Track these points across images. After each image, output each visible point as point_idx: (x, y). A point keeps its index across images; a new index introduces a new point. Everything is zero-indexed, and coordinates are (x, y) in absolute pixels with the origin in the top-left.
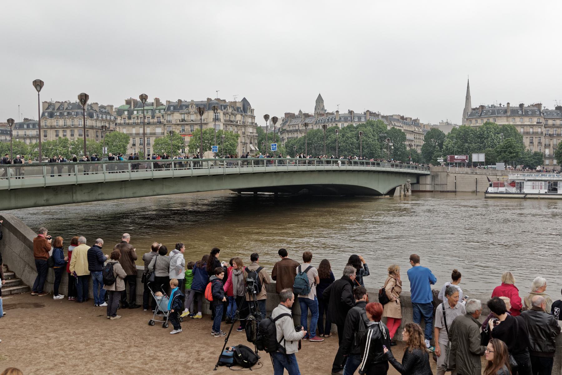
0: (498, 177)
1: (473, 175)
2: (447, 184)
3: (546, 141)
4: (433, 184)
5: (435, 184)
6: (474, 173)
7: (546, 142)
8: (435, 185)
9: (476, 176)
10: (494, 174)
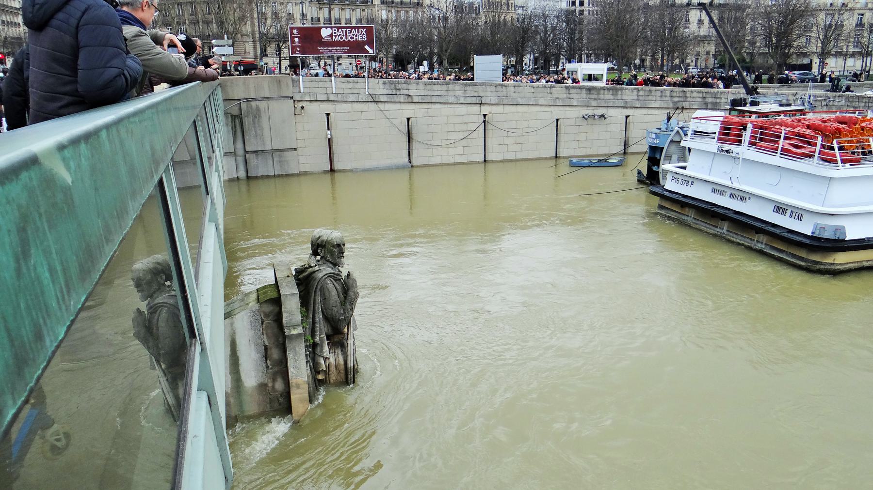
0: (485, 110)
1: (398, 106)
2: (295, 149)
3: (313, 10)
4: (240, 152)
5: (246, 152)
6: (402, 99)
7: (313, 14)
8: (251, 157)
9: (408, 110)
10: (474, 100)
